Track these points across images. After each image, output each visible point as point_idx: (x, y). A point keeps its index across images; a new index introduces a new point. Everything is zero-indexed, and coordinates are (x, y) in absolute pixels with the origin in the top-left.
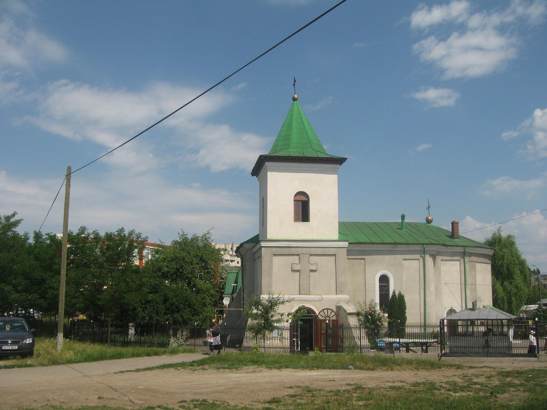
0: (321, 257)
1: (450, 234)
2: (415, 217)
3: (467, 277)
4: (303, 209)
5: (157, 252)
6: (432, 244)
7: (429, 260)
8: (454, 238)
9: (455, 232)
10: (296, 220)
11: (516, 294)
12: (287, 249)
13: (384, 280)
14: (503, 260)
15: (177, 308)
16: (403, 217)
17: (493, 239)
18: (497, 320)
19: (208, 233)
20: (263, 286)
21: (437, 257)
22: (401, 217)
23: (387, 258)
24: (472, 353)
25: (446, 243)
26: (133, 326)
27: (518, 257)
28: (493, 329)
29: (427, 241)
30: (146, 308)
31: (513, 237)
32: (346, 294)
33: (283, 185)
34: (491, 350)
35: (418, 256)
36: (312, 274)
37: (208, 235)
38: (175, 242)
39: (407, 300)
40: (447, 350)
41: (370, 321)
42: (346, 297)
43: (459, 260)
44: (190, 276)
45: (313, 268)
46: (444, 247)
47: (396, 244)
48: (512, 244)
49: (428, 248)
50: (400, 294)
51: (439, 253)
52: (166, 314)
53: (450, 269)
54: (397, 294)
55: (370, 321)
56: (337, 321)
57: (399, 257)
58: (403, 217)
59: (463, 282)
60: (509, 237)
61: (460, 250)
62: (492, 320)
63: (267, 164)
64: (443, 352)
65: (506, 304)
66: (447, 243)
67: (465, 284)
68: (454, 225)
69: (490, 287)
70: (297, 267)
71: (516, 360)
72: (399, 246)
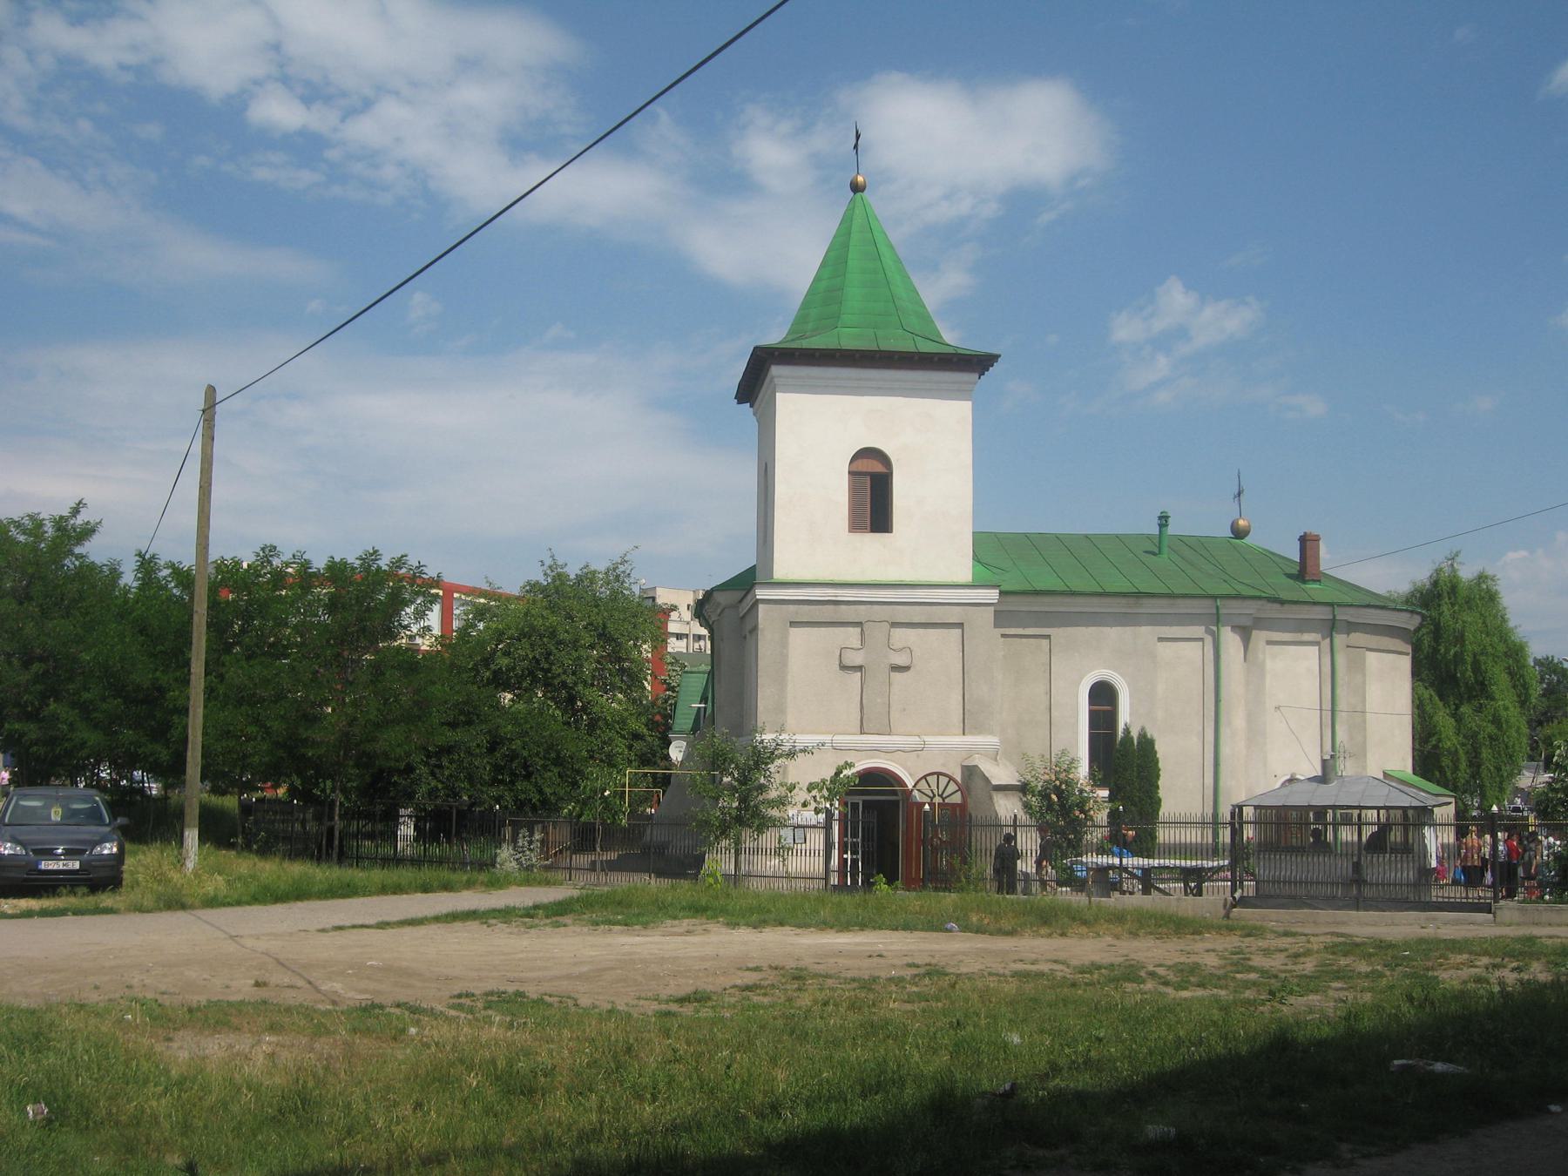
0: (921, 631)
1: (1295, 570)
2: (1201, 517)
3: (1338, 691)
4: (873, 496)
5: (481, 613)
7: (1231, 641)
8: (1304, 582)
9: (1309, 562)
10: (855, 526)
12: (830, 607)
13: (1103, 695)
14: (1451, 644)
15: (526, 766)
16: (1163, 520)
17: (1435, 584)
18: (1387, 808)
20: (760, 708)
21: (1255, 633)
22: (1156, 521)
23: (1113, 633)
25: (1285, 593)
26: (410, 817)
27: (1503, 634)
28: (1395, 834)
29: (1225, 589)
30: (440, 767)
32: (992, 733)
33: (820, 428)
34: (1368, 892)
35: (1199, 631)
36: (896, 676)
38: (533, 587)
39: (1164, 751)
44: (570, 680)
45: (900, 660)
46: (1277, 606)
47: (1139, 595)
48: (1492, 597)
49: (1228, 608)
50: (1142, 735)
51: (1260, 623)
52: (495, 782)
53: (1292, 669)
54: (1135, 734)
56: (962, 807)
58: (1163, 520)
59: (1327, 705)
60: (1482, 578)
61: (1321, 613)
62: (1378, 808)
63: (776, 370)
64: (1237, 895)
65: (1463, 765)
66: (1284, 595)
68: (1307, 543)
70: (856, 659)
71: (1435, 919)
72: (1145, 601)
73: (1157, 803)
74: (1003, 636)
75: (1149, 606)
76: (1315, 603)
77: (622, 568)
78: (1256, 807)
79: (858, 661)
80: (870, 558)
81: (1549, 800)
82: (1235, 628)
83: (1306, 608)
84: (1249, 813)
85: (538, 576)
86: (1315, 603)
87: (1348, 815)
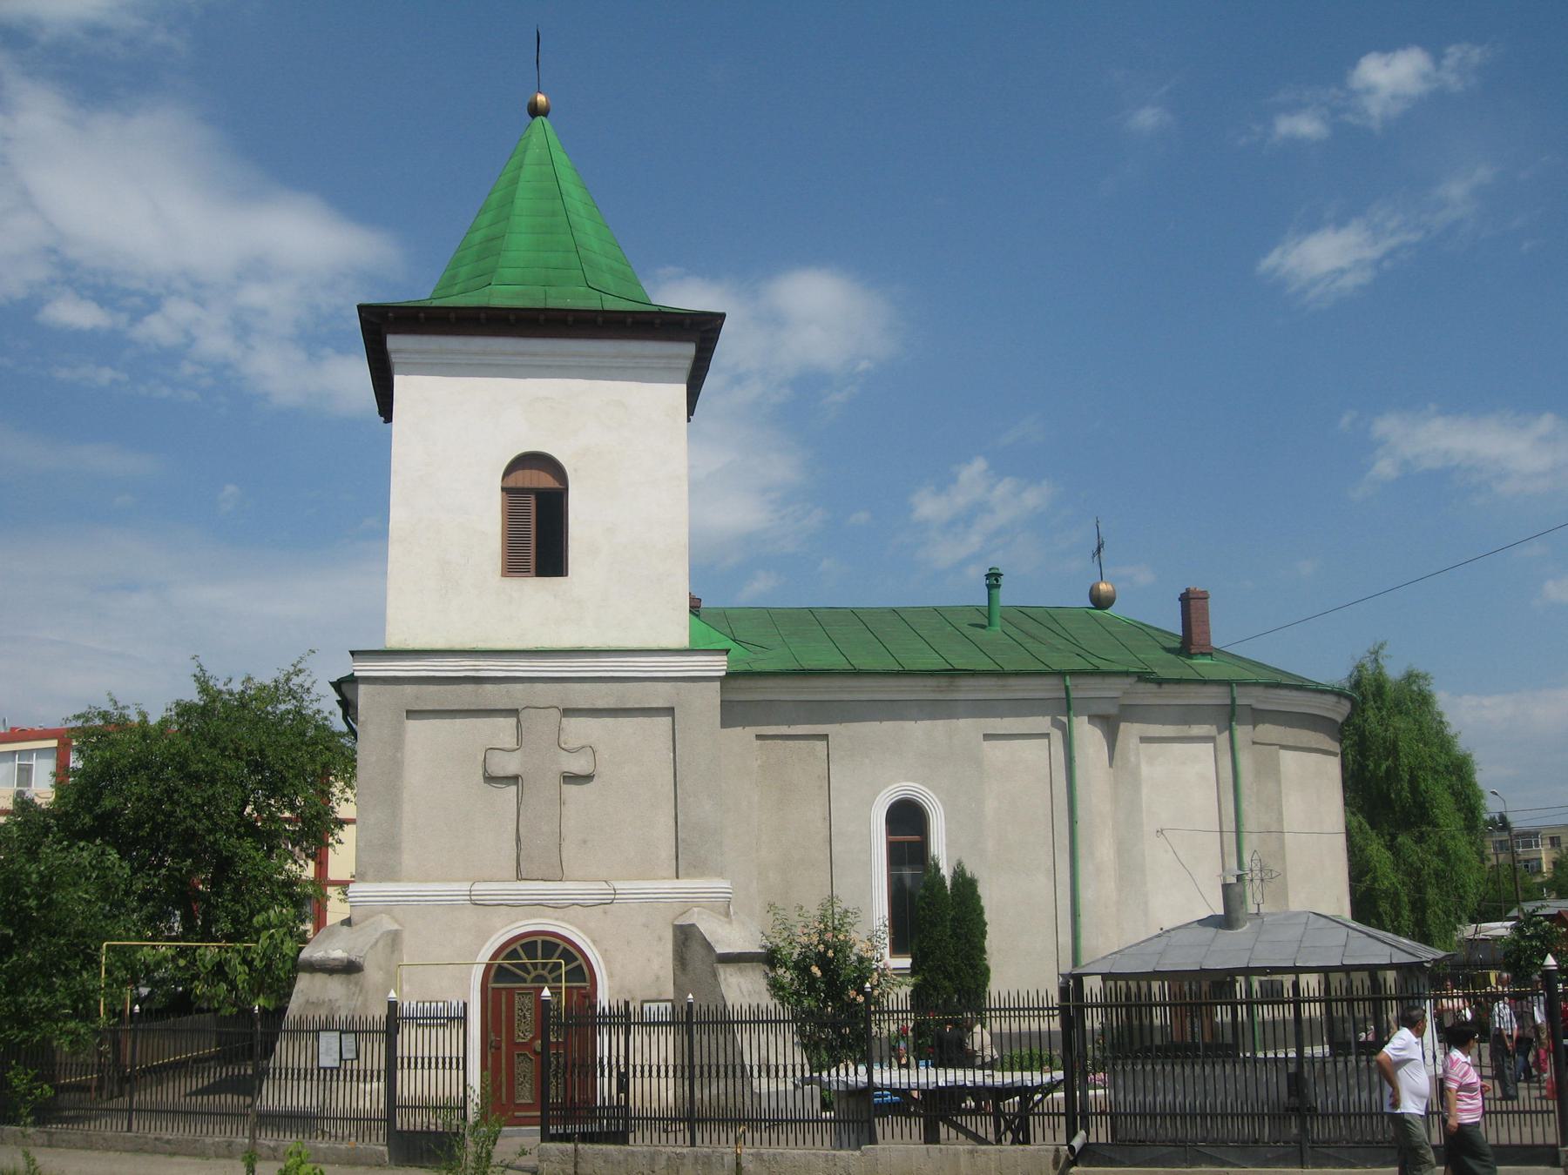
0: (609, 721)
2: (1047, 579)
3: (1244, 805)
4: (539, 524)
6: (1097, 673)
7: (1088, 736)
8: (1190, 656)
9: (1195, 630)
10: (513, 566)
11: (1437, 874)
12: (464, 687)
13: (907, 820)
16: (993, 579)
18: (1347, 969)
19: (298, 672)
21: (1123, 726)
22: (984, 581)
23: (918, 731)
24: (1224, 1142)
25: (1164, 673)
27: (1445, 744)
29: (1078, 664)
31: (1425, 678)
32: (721, 874)
33: (460, 426)
34: (1318, 1130)
35: (1042, 723)
36: (571, 790)
37: (296, 680)
38: (185, 710)
39: (990, 896)
40: (1100, 1133)
41: (823, 995)
42: (720, 884)
43: (1211, 739)
45: (578, 765)
46: (1152, 687)
47: (953, 673)
48: (1425, 700)
49: (1084, 689)
51: (1130, 713)
55: (823, 995)
57: (967, 728)
58: (993, 579)
59: (1230, 825)
60: (1411, 677)
61: (1214, 696)
62: (1325, 971)
63: (394, 342)
64: (1077, 1142)
65: (1406, 913)
67: (1238, 832)
68: (1190, 603)
69: (1340, 842)
70: (510, 765)
73: (985, 973)
74: (759, 737)
75: (968, 690)
76: (1205, 682)
77: (296, 680)
78: (1106, 977)
79: (511, 769)
80: (534, 613)
81: (1520, 950)
82: (1093, 718)
83: (1192, 688)
84: (1093, 985)
85: (193, 696)
86: (1205, 682)
87: (1272, 984)
